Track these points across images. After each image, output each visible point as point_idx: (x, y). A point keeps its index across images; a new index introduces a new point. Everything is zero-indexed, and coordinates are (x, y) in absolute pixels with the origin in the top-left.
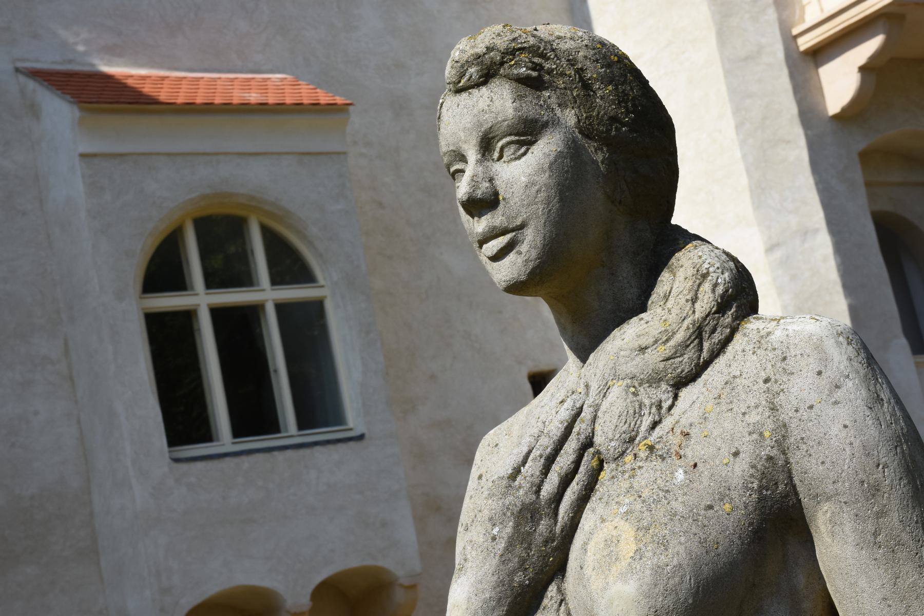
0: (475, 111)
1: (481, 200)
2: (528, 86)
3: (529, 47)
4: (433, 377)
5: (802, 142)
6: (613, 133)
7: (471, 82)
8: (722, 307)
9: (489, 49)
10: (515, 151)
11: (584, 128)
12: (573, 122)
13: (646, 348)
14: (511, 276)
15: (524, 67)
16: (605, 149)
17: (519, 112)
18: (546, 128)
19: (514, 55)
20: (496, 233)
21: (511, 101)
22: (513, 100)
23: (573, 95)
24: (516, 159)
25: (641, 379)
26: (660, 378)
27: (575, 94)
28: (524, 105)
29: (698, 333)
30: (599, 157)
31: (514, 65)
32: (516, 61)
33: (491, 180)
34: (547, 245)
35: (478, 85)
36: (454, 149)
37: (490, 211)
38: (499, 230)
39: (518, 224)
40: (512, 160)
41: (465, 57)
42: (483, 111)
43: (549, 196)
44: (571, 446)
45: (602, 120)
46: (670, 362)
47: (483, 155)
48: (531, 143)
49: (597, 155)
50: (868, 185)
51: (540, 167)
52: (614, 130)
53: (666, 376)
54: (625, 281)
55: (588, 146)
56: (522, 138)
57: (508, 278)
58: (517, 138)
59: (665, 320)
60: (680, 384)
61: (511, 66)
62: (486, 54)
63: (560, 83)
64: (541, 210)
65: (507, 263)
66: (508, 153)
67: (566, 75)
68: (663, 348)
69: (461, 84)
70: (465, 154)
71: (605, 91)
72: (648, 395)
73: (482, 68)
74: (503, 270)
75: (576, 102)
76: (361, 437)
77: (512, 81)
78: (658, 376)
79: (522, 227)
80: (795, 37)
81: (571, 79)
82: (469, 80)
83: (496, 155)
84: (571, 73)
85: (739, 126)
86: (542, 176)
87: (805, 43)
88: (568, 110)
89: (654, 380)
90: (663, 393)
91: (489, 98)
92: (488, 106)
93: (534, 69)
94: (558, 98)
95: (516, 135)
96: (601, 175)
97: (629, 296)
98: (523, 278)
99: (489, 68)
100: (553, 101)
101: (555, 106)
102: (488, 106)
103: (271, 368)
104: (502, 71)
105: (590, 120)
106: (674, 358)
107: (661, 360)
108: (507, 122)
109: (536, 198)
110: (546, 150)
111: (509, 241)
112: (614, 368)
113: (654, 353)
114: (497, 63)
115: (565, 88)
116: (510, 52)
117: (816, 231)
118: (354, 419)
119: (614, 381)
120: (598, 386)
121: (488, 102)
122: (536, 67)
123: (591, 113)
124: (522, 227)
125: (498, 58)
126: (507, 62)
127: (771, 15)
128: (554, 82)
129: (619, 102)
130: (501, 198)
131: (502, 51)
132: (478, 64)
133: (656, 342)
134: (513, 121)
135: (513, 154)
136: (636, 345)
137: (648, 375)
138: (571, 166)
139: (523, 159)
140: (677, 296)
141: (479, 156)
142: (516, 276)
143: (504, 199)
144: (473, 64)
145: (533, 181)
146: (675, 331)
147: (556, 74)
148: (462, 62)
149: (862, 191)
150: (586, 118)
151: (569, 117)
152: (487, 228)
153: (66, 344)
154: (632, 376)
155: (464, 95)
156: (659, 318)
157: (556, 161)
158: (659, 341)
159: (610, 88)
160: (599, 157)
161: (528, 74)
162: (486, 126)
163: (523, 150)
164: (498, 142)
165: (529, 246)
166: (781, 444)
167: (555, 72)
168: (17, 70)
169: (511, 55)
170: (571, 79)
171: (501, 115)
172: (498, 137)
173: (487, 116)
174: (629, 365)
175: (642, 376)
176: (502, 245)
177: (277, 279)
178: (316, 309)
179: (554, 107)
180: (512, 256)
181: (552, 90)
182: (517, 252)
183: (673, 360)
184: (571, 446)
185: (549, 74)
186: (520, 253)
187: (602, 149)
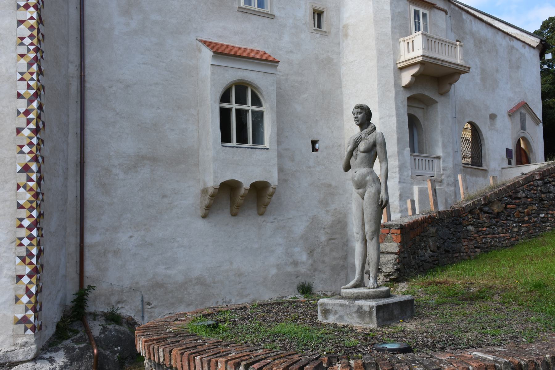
4: (287, 137)
5: (394, 92)
8: (373, 129)
29: (371, 131)
44: (360, 138)
50: (408, 106)
60: (369, 134)
72: (366, 135)
76: (268, 149)
85: (378, 84)
87: (400, 66)
89: (367, 134)
90: (368, 135)
103: (248, 127)
117: (393, 116)
118: (267, 144)
127: (392, 56)
149: (406, 107)
151: (364, 112)
153: (198, 112)
166: (376, 140)
168: (197, 39)
177: (253, 104)
178: (262, 113)
184: (360, 138)
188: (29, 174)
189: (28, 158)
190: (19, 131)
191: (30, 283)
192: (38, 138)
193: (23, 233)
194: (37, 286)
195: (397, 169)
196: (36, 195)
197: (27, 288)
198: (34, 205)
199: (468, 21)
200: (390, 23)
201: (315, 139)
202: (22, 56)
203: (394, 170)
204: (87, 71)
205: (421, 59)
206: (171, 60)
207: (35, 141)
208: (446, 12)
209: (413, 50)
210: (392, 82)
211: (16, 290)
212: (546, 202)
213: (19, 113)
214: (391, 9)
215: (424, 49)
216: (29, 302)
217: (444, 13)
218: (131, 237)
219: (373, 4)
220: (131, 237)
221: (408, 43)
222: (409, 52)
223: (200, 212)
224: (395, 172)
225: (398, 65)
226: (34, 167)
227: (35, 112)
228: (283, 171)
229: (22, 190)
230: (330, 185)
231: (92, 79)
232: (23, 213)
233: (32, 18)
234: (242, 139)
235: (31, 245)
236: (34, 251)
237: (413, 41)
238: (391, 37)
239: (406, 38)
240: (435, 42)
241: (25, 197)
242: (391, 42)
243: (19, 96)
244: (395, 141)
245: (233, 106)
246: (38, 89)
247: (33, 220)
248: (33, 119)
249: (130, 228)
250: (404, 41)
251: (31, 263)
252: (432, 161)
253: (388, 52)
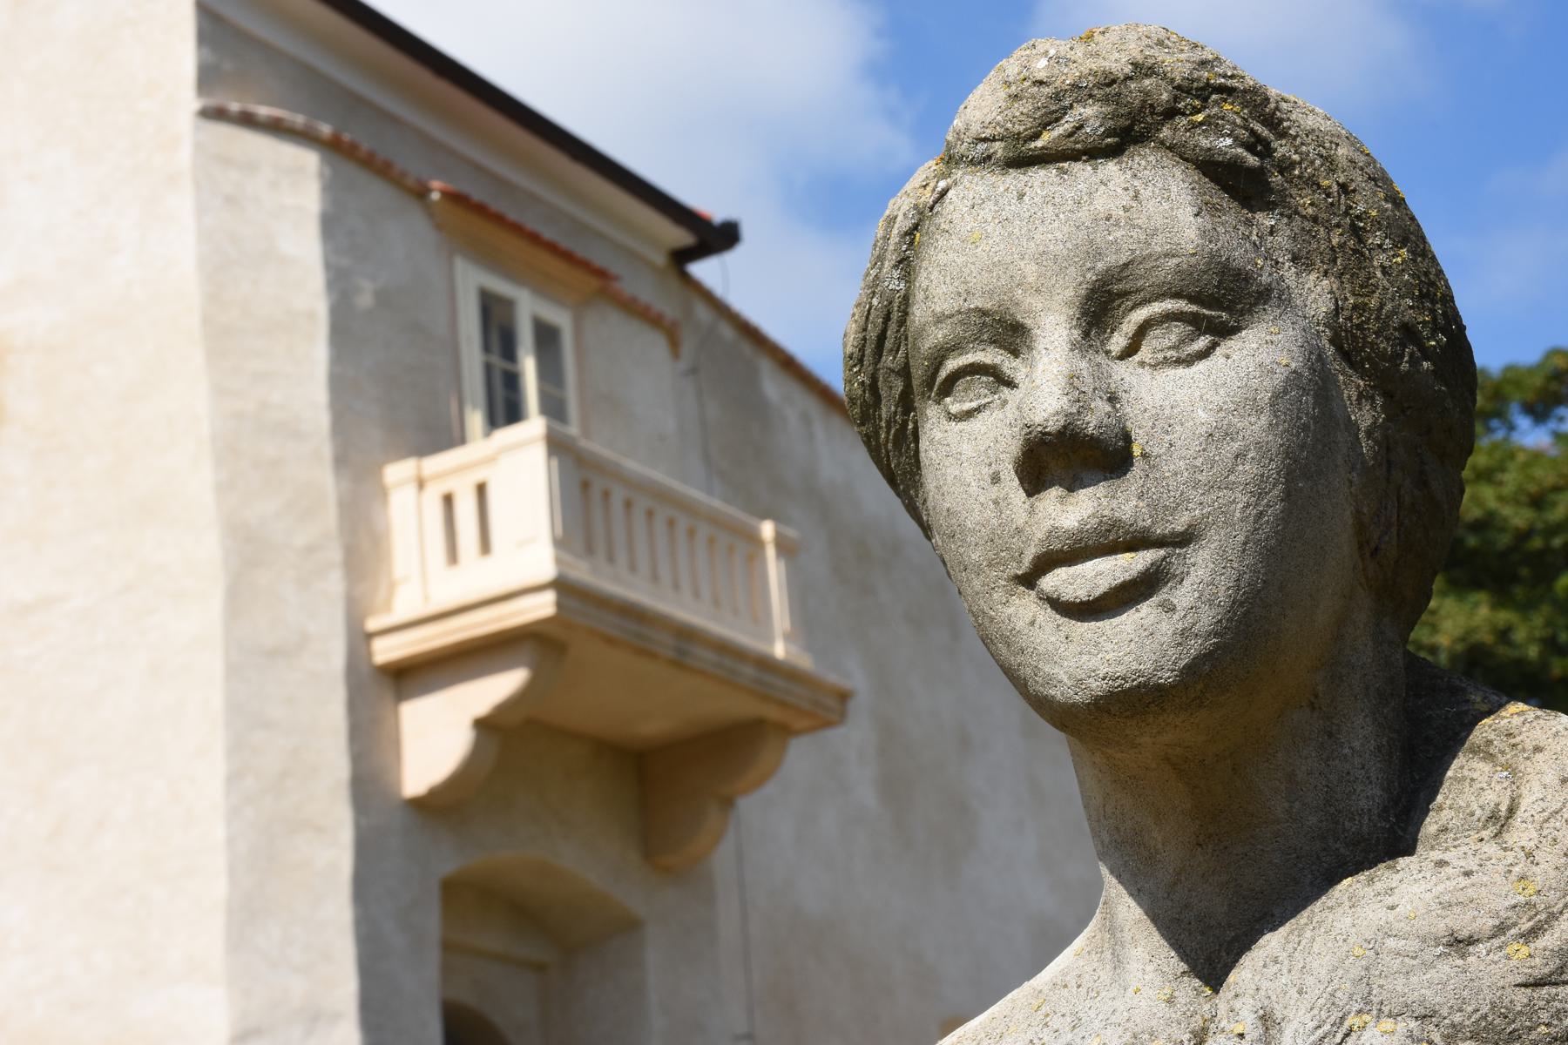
0: (1084, 215)
1: (1094, 443)
2: (1225, 188)
3: (1245, 91)
6: (1404, 366)
7: (1076, 142)
9: (1142, 69)
10: (1182, 342)
11: (1346, 331)
12: (1324, 309)
13: (1471, 941)
14: (1135, 666)
15: (1229, 135)
16: (1379, 401)
17: (1210, 242)
18: (1265, 304)
19: (1205, 100)
20: (1115, 541)
21: (1190, 210)
22: (1196, 210)
23: (1330, 241)
24: (1179, 362)
25: (1453, 1026)
26: (1515, 1030)
27: (1335, 241)
28: (1221, 229)
30: (1364, 417)
31: (1201, 124)
32: (1209, 116)
33: (1113, 399)
34: (1241, 604)
35: (1094, 153)
36: (988, 306)
37: (1105, 479)
38: (1127, 532)
39: (1180, 528)
40: (1167, 362)
41: (1069, 75)
42: (1108, 219)
43: (1262, 476)
45: (1386, 326)
46: (1545, 991)
47: (1086, 335)
48: (1224, 331)
49: (1360, 409)
50: (447, 947)
51: (1250, 395)
52: (1406, 359)
53: (1530, 1029)
54: (1357, 761)
55: (1344, 383)
56: (1207, 312)
57: (1121, 670)
58: (1194, 308)
59: (1522, 878)
61: (1195, 125)
62: (1131, 78)
63: (1305, 201)
64: (1240, 506)
65: (1129, 628)
66: (1159, 342)
67: (1319, 186)
68: (1525, 950)
69: (1039, 143)
70: (1028, 322)
71: (1393, 256)
73: (1116, 110)
74: (1108, 646)
75: (1334, 261)
77: (1189, 165)
78: (1509, 1024)
79: (1183, 540)
80: (370, 636)
81: (1330, 200)
82: (1071, 135)
83: (1118, 342)
84: (1330, 187)
85: (233, 779)
86: (1253, 419)
87: (387, 651)
88: (1313, 276)
91: (1126, 189)
92: (1126, 209)
93: (1250, 148)
94: (1294, 239)
95: (1191, 299)
96: (1358, 466)
97: (1363, 803)
98: (1166, 677)
99: (1135, 116)
100: (1282, 239)
101: (1284, 258)
102: (1126, 209)
104: (1165, 132)
105: (1361, 315)
106: (1556, 984)
107: (1519, 981)
108: (1175, 261)
109: (1232, 471)
110: (1265, 357)
111: (1148, 569)
112: (1365, 980)
113: (1496, 958)
114: (1159, 109)
115: (1315, 219)
116: (1197, 89)
119: (1366, 1017)
120: (1315, 1023)
121: (1126, 200)
122: (1256, 144)
123: (1366, 300)
124: (1183, 540)
125: (1165, 96)
126: (1184, 114)
127: (335, 584)
128: (1291, 196)
129: (1422, 296)
130: (1137, 451)
131: (1178, 80)
132: (1106, 100)
133: (1501, 929)
134: (1193, 260)
135: (1175, 347)
136: (1441, 927)
137: (1478, 1015)
138: (1314, 418)
139: (1201, 366)
140: (1547, 821)
141: (1076, 333)
142: (1147, 667)
143: (1144, 456)
144: (1091, 96)
145: (1229, 425)
146: (1555, 910)
147: (1300, 177)
148: (1058, 84)
149: (433, 957)
150: (1355, 307)
152: (1094, 521)
154: (1423, 1012)
155: (1040, 178)
156: (1501, 868)
157: (1285, 392)
158: (1509, 928)
159: (1404, 251)
160: (1364, 417)
161: (1237, 156)
162: (1112, 259)
163: (1202, 342)
164: (1133, 308)
165: (1196, 595)
167: (1297, 172)
169: (1197, 97)
170: (1330, 200)
171: (1160, 239)
172: (1139, 297)
173: (1119, 234)
174: (1414, 979)
175: (1457, 1018)
176: (1127, 576)
179: (1281, 260)
180: (1146, 612)
181: (1282, 214)
182: (1161, 605)
183: (1553, 990)
185: (1281, 173)
186: (1169, 608)
187: (1372, 399)
205: (543, 606)
208: (674, 344)
209: (485, 546)
210: (336, 765)
215: (560, 543)
217: (655, 344)
221: (448, 500)
222: (453, 555)
237: (481, 490)
238: (327, 451)
240: (628, 505)
250: (421, 484)
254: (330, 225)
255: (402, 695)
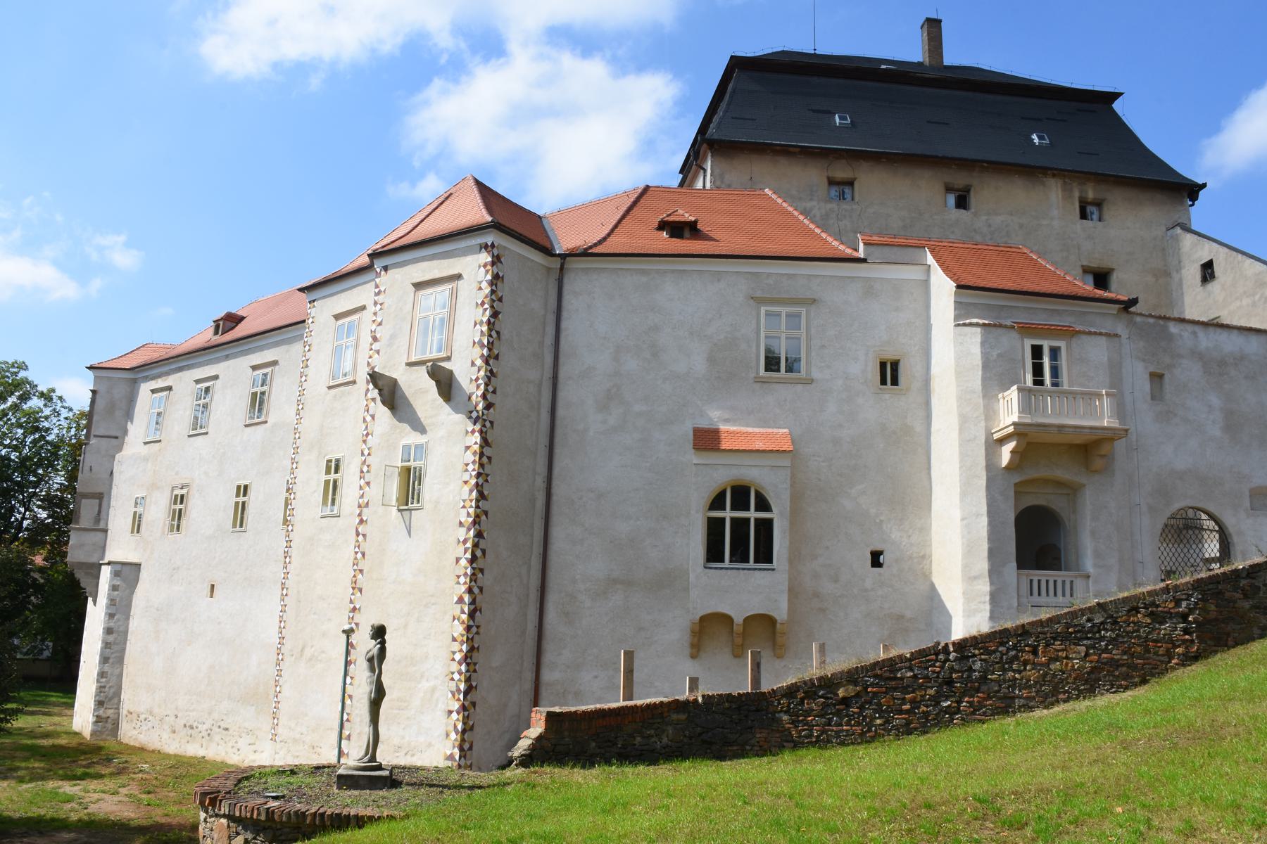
4: (827, 548)
5: (985, 478)
80: (993, 434)
85: (961, 467)
87: (996, 436)
117: (982, 515)
127: (983, 424)
177: (757, 510)
188: (463, 606)
189: (464, 588)
190: (458, 560)
191: (458, 720)
192: (473, 568)
193: (455, 667)
194: (464, 723)
195: (988, 598)
196: (468, 629)
197: (455, 724)
198: (465, 639)
199: (1186, 335)
200: (980, 373)
201: (878, 548)
202: (466, 482)
203: (983, 600)
204: (555, 482)
205: (1011, 429)
206: (657, 458)
207: (469, 571)
210: (983, 462)
211: (447, 725)
212: (958, 685)
213: (459, 541)
214: (982, 353)
216: (456, 740)
218: (596, 677)
219: (955, 347)
220: (596, 677)
223: (687, 651)
224: (985, 603)
225: (994, 435)
226: (467, 598)
227: (471, 541)
228: (818, 597)
229: (456, 621)
230: (900, 617)
231: (559, 490)
232: (456, 647)
233: (476, 443)
234: (740, 555)
235: (459, 680)
236: (462, 687)
238: (981, 395)
239: (1006, 394)
241: (459, 629)
242: (981, 401)
243: (461, 524)
244: (986, 554)
245: (728, 514)
246: (477, 516)
247: (463, 654)
248: (469, 548)
249: (596, 666)
251: (459, 700)
252: (1072, 582)
253: (977, 417)
254: (983, 344)
255: (1001, 446)
